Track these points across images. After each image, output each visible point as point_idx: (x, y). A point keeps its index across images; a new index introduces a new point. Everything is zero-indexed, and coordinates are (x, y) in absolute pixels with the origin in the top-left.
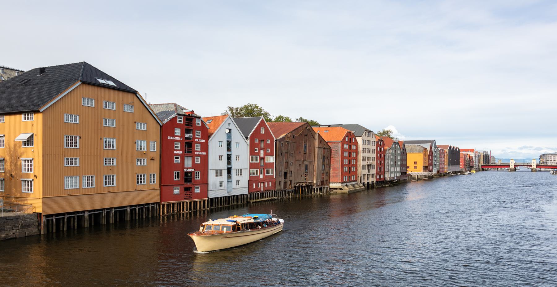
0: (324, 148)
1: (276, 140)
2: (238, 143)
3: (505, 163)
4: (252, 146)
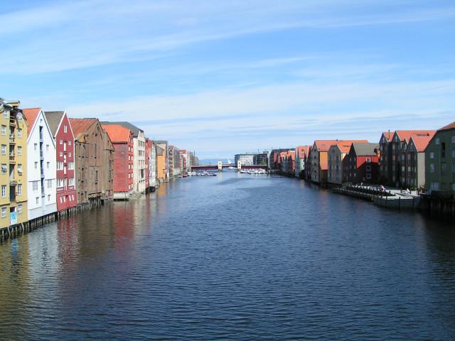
0: (111, 151)
1: (76, 141)
2: (48, 146)
3: (213, 164)
4: (59, 148)
